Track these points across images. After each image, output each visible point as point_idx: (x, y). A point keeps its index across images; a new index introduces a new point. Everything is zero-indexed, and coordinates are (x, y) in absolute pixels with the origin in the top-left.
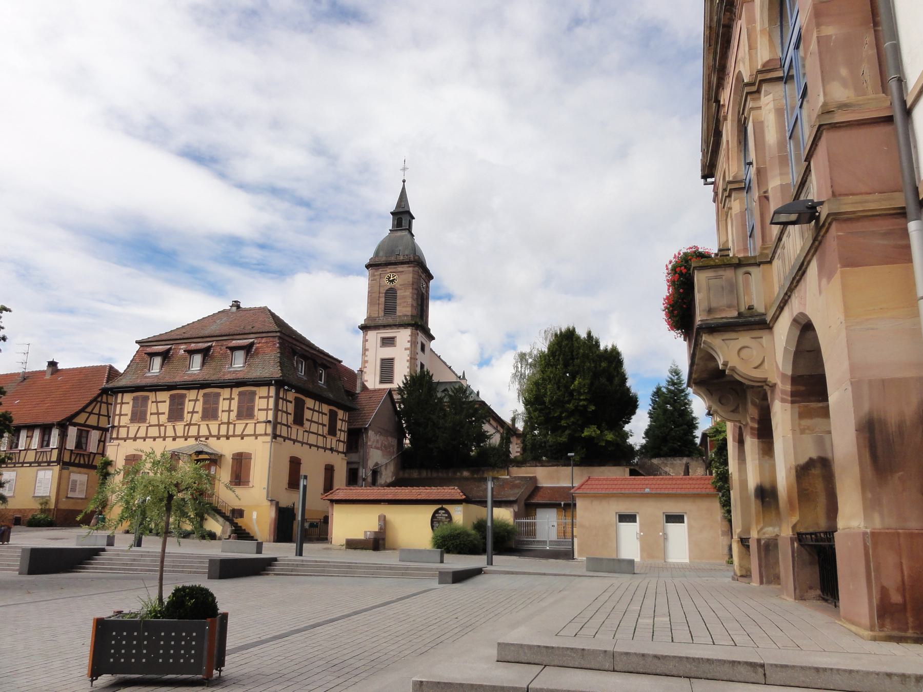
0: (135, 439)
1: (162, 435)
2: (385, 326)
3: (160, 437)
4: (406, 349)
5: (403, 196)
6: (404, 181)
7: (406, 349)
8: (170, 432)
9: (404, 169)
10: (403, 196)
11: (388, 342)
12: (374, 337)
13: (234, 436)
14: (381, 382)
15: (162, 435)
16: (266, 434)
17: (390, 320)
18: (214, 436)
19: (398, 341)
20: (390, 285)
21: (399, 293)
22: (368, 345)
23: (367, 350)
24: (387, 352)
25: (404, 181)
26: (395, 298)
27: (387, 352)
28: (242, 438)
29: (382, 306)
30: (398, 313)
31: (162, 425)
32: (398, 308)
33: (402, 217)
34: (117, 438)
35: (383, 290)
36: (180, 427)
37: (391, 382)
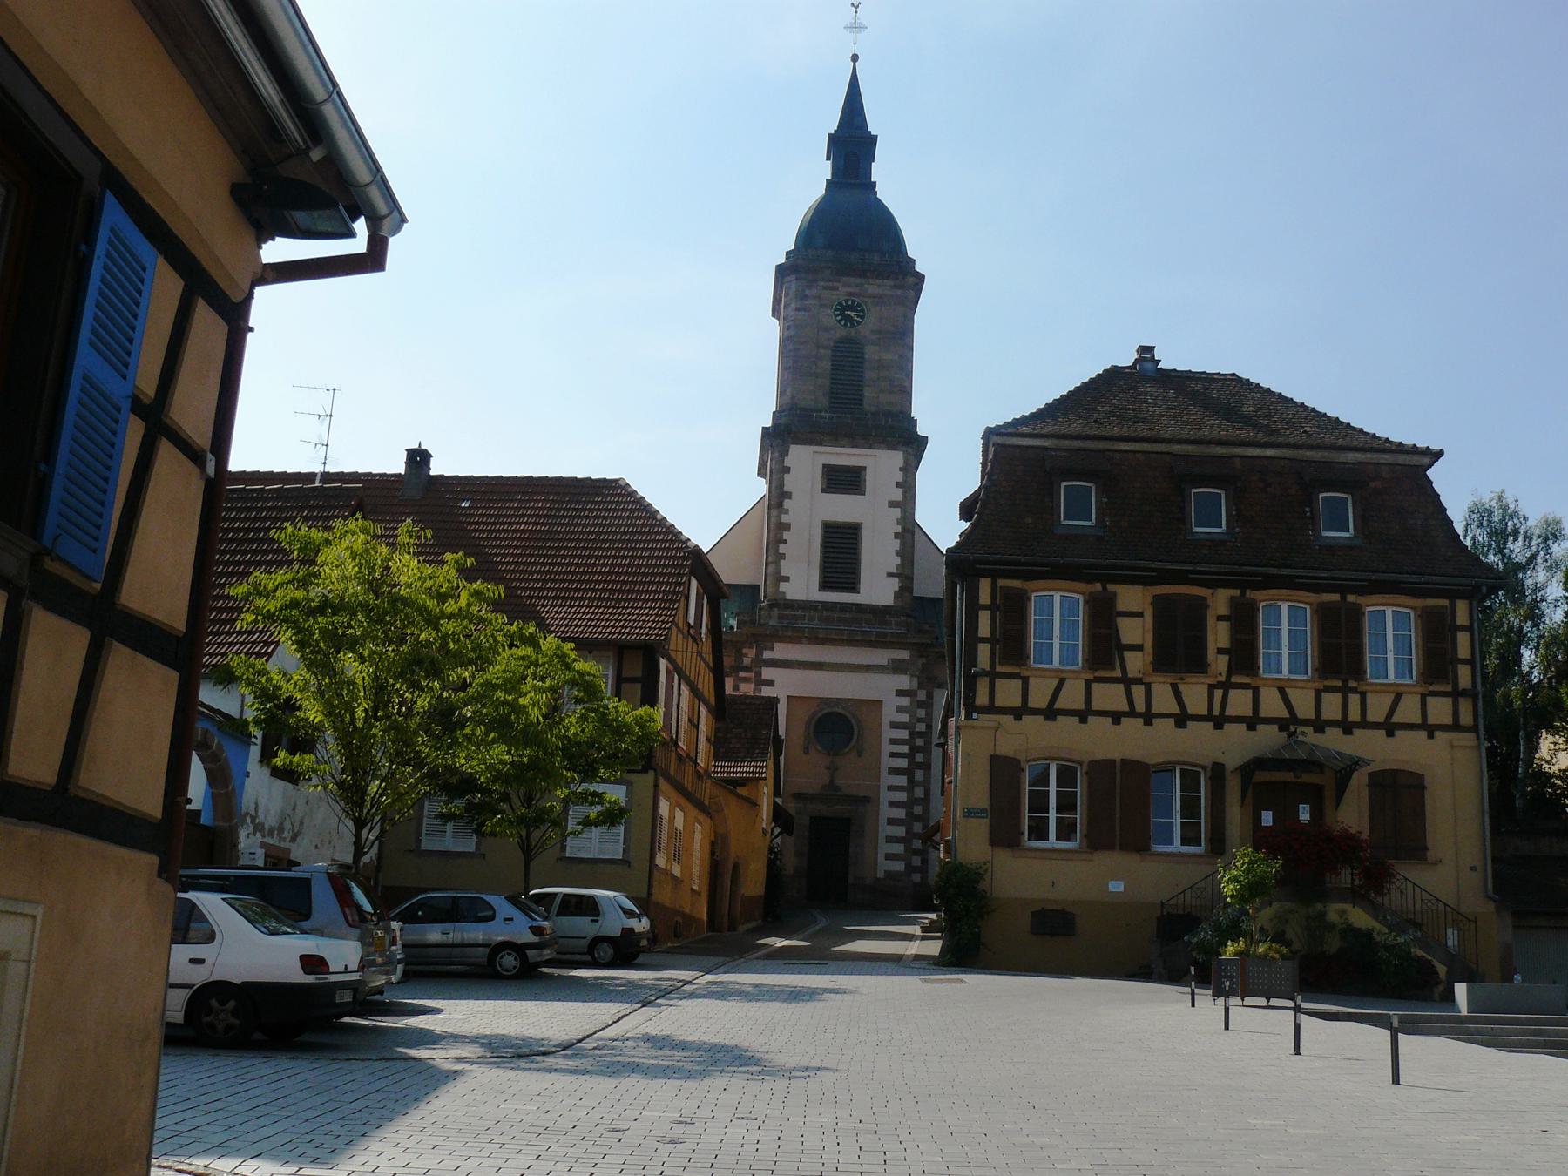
0: (1050, 713)
1: (1140, 706)
3: (1132, 713)
4: (892, 504)
6: (855, 58)
7: (892, 504)
8: (1163, 699)
9: (856, 28)
11: (843, 480)
12: (806, 461)
13: (1364, 724)
14: (825, 585)
15: (1140, 706)
16: (1456, 726)
18: (1140, 715)
20: (841, 332)
21: (870, 352)
22: (790, 483)
23: (789, 495)
24: (842, 508)
25: (855, 58)
27: (842, 508)
28: (1390, 734)
31: (1138, 681)
32: (868, 393)
33: (852, 146)
34: (991, 709)
36: (1196, 695)
37: (853, 587)
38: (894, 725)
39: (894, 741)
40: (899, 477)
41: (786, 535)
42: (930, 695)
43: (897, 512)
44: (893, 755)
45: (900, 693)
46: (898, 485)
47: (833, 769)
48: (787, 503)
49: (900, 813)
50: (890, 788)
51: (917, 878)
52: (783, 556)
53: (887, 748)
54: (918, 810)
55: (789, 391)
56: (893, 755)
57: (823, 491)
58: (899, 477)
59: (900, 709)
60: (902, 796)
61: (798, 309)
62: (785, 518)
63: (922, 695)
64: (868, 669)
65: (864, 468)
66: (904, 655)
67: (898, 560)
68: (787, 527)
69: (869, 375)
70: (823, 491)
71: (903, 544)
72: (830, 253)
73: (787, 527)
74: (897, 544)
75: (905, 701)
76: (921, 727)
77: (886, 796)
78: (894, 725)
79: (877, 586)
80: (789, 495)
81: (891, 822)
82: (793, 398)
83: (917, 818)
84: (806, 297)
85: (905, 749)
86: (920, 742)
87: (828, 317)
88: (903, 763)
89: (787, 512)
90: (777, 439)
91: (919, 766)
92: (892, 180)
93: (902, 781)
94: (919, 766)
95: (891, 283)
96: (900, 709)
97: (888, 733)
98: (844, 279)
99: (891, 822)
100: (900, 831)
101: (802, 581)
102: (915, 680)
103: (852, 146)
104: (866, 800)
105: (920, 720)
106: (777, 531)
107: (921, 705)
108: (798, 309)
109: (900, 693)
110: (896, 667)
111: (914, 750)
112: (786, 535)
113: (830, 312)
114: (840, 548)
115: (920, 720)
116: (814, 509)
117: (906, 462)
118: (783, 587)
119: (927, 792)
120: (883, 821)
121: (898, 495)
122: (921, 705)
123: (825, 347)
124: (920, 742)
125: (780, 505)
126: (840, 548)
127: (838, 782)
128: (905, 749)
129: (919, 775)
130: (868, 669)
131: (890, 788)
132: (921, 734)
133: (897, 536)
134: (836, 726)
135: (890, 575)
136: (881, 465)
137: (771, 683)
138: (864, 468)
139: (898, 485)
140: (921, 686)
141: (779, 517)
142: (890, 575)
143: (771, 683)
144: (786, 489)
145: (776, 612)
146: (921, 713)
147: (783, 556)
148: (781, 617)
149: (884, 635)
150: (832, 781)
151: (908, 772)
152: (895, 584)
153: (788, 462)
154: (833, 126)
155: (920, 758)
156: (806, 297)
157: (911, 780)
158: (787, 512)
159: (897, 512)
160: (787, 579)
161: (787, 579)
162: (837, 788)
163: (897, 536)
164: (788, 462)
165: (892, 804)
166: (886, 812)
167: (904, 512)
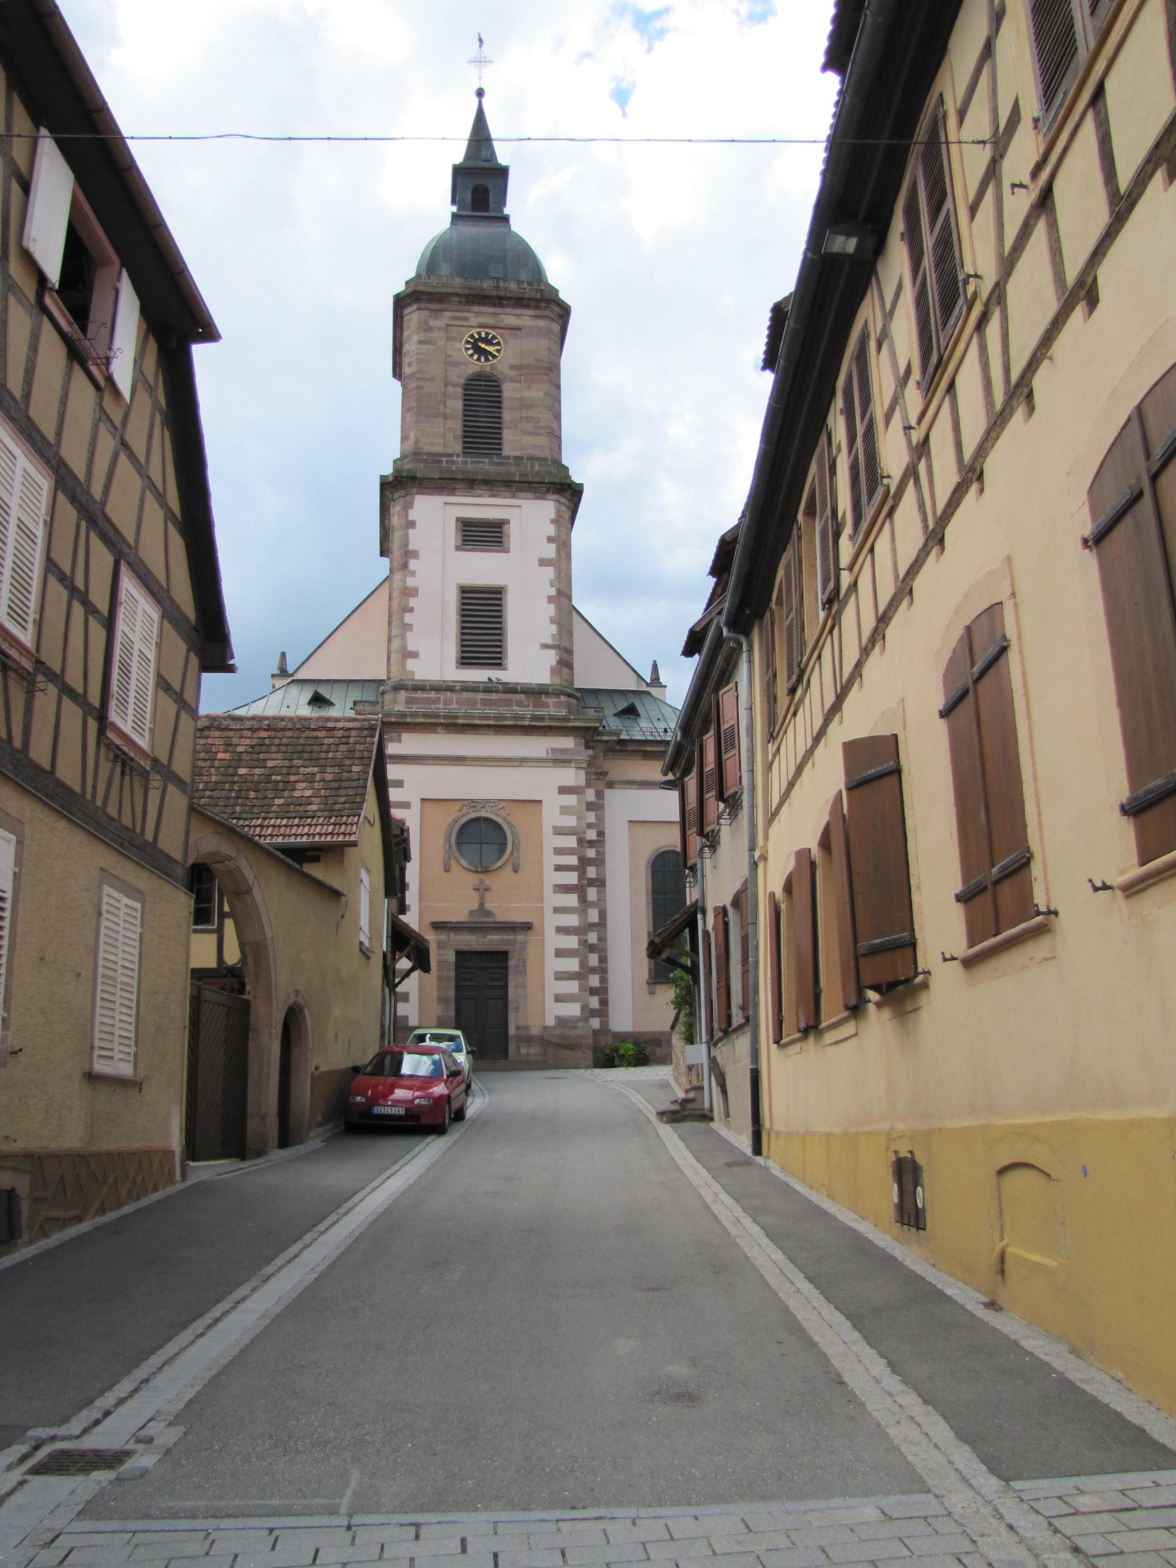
2: (473, 483)
4: (543, 562)
5: (480, 136)
6: (480, 93)
7: (543, 562)
10: (480, 136)
11: (482, 535)
12: (433, 517)
14: (466, 659)
17: (486, 466)
19: (514, 534)
20: (476, 365)
24: (482, 568)
25: (480, 93)
26: (496, 403)
27: (482, 568)
29: (457, 425)
30: (508, 450)
32: (507, 435)
33: (480, 183)
35: (459, 376)
37: (496, 659)
38: (559, 831)
39: (559, 851)
40: (551, 530)
41: (412, 602)
42: (600, 795)
43: (550, 572)
44: (559, 868)
45: (563, 790)
46: (550, 540)
47: (482, 890)
48: (413, 564)
49: (572, 942)
50: (557, 910)
51: (595, 1023)
52: (408, 627)
53: (550, 860)
54: (593, 938)
55: (412, 435)
56: (559, 868)
57: (458, 548)
58: (551, 530)
59: (565, 810)
60: (573, 920)
61: (421, 342)
62: (411, 582)
63: (590, 795)
64: (522, 761)
65: (507, 522)
66: (567, 743)
67: (554, 629)
68: (413, 592)
69: (507, 415)
70: (458, 548)
71: (559, 609)
72: (458, 281)
73: (413, 592)
74: (551, 610)
75: (571, 800)
76: (592, 835)
77: (552, 921)
78: (559, 831)
79: (527, 661)
80: (415, 554)
81: (560, 953)
82: (417, 442)
83: (592, 948)
84: (430, 329)
85: (573, 860)
86: (591, 853)
87: (461, 351)
88: (572, 878)
89: (413, 574)
90: (397, 487)
91: (591, 883)
92: (527, 211)
93: (572, 900)
94: (591, 883)
95: (532, 312)
96: (565, 810)
97: (553, 841)
98: (476, 308)
99: (560, 953)
100: (573, 965)
101: (436, 657)
102: (582, 773)
103: (480, 183)
104: (527, 927)
105: (590, 826)
106: (398, 598)
107: (590, 807)
108: (421, 342)
109: (563, 790)
110: (559, 760)
111: (584, 862)
112: (412, 602)
113: (463, 345)
114: (482, 617)
115: (590, 826)
116: (444, 571)
117: (558, 513)
118: (411, 664)
119: (603, 914)
120: (549, 953)
121: (550, 551)
122: (590, 807)
123: (454, 385)
124: (591, 853)
125: (405, 566)
126: (482, 617)
127: (489, 906)
128: (573, 860)
129: (592, 894)
130: (522, 761)
131: (557, 910)
132: (591, 844)
133: (550, 599)
134: (482, 836)
135: (546, 646)
136: (529, 519)
137: (399, 784)
138: (507, 522)
139: (550, 540)
140: (589, 784)
141: (404, 581)
142: (546, 646)
143: (399, 784)
144: (411, 547)
145: (403, 695)
146: (591, 817)
147: (408, 627)
148: (409, 701)
149: (541, 718)
150: (482, 905)
151: (579, 890)
152: (551, 657)
153: (413, 515)
154: (459, 157)
155: (591, 872)
156: (430, 329)
157: (583, 899)
158: (413, 574)
159: (550, 572)
160: (415, 655)
161: (415, 655)
162: (488, 913)
163: (550, 599)
164: (413, 515)
165: (560, 930)
166: (553, 941)
167: (558, 571)
